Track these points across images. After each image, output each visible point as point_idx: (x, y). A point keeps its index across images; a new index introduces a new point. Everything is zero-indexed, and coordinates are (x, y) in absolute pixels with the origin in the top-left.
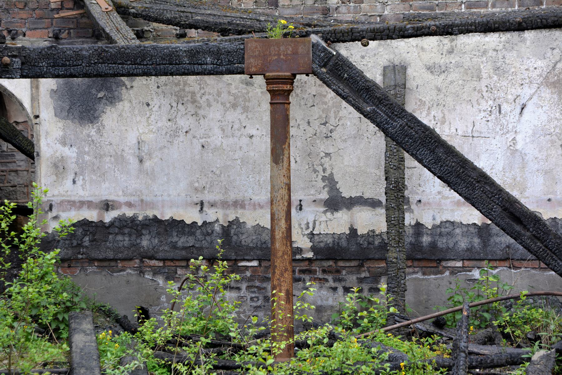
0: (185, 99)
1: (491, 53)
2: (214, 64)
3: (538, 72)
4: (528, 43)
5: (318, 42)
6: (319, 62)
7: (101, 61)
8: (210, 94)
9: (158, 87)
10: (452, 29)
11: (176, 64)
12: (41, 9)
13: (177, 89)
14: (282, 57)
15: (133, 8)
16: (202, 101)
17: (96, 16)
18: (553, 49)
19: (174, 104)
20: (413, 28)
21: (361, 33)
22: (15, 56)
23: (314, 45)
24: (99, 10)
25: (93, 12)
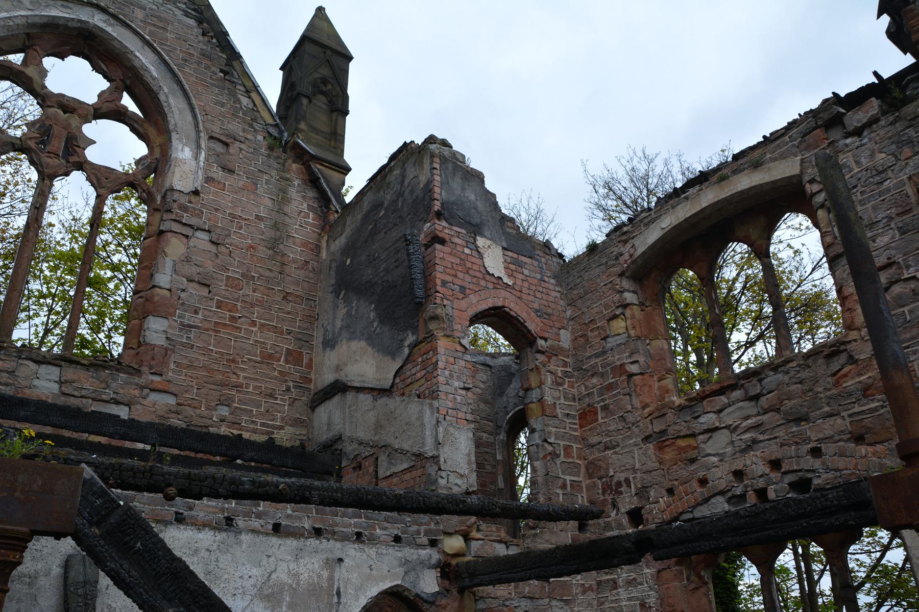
1: (204, 553)
3: (252, 581)
4: (244, 546)
5: (93, 478)
6: (90, 515)
10: (310, 493)
14: (18, 494)
18: (269, 556)
20: (253, 482)
21: (167, 477)
23: (85, 482)
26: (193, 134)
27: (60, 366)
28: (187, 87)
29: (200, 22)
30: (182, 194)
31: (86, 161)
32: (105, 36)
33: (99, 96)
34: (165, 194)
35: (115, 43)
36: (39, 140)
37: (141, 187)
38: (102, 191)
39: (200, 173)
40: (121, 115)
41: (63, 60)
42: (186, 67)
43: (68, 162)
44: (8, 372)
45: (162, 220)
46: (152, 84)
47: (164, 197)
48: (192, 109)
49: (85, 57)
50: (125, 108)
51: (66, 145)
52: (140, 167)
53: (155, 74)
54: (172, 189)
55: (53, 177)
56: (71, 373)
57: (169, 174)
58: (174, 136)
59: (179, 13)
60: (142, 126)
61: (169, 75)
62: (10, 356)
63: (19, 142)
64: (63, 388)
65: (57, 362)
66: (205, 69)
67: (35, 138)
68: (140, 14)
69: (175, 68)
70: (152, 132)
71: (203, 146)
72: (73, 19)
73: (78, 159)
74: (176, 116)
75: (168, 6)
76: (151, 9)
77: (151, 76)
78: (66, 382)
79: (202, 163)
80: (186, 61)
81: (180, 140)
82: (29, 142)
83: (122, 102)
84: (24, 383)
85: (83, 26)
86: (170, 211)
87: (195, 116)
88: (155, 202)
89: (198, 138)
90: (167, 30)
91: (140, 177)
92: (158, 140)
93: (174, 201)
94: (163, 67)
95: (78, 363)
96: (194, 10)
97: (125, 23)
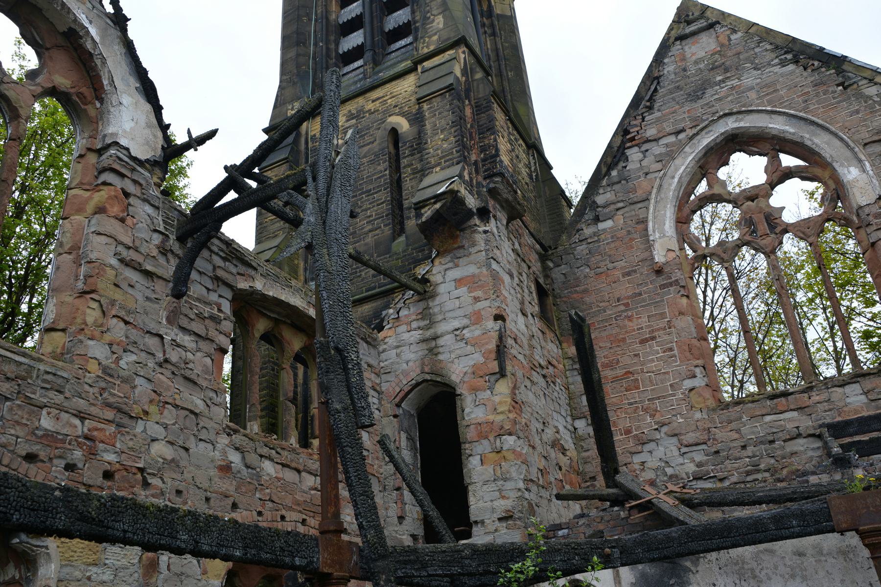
0: (746, 576)
2: (800, 526)
7: (690, 540)
8: (767, 568)
9: (720, 568)
11: (763, 532)
12: (614, 520)
13: (737, 568)
15: (696, 499)
16: (762, 575)
17: (667, 510)
19: (738, 582)
22: (614, 547)
24: (667, 505)
25: (663, 508)
26: (848, 153)
27: (858, 382)
28: (820, 122)
29: (796, 61)
30: (870, 206)
31: (788, 225)
32: (742, 131)
33: (766, 172)
34: (858, 213)
35: (752, 130)
36: (750, 232)
37: (836, 218)
38: (811, 239)
39: (875, 181)
40: (789, 174)
41: (728, 164)
42: (810, 106)
43: (777, 234)
44: (826, 401)
45: (868, 235)
46: (795, 138)
47: (858, 215)
48: (836, 135)
49: (740, 151)
50: (788, 168)
51: (767, 223)
52: (826, 203)
53: (792, 130)
54: (861, 207)
55: (773, 252)
56: (868, 383)
57: (851, 196)
58: (835, 164)
59: (777, 69)
60: (807, 172)
61: (802, 123)
62: (821, 390)
63: (740, 242)
64: (869, 397)
65: (854, 380)
66: (824, 95)
67: (747, 232)
68: (752, 95)
69: (801, 114)
70: (818, 171)
71: (863, 158)
72: (717, 137)
73: (781, 228)
74: (828, 150)
75: (767, 71)
76: (757, 84)
77: (790, 133)
78: (869, 391)
79: (871, 172)
80: (806, 101)
81: (842, 165)
82: (745, 238)
83: (784, 165)
84: (841, 404)
85: (726, 135)
86: (869, 225)
87: (841, 139)
88: (854, 223)
89: (855, 154)
90: (778, 90)
91: (831, 211)
92: (826, 175)
93: (868, 215)
94: (794, 121)
95: (869, 374)
96: (786, 53)
97: (748, 111)
